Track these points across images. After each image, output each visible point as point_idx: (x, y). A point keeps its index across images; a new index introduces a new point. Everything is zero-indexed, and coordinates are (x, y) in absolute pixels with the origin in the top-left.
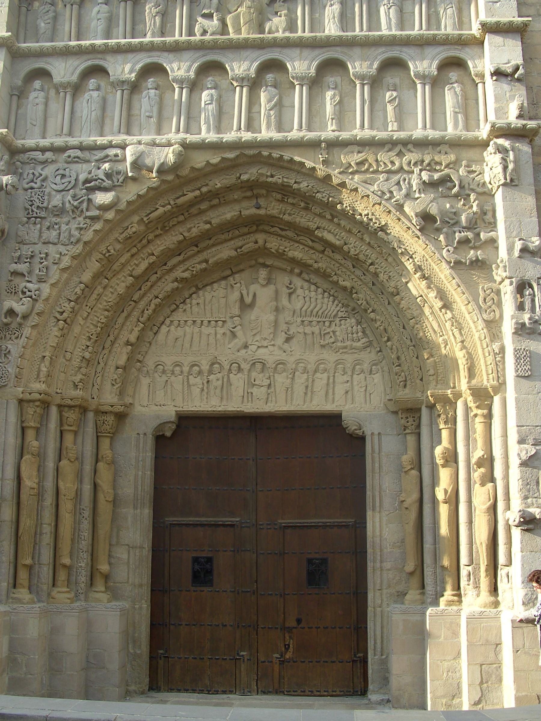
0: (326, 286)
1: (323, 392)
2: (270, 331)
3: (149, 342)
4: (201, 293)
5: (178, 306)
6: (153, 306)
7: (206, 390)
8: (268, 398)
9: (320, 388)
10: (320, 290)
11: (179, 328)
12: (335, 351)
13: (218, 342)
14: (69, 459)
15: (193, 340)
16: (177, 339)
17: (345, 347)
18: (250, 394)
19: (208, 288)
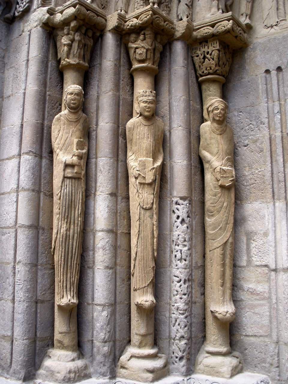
14: (141, 115)
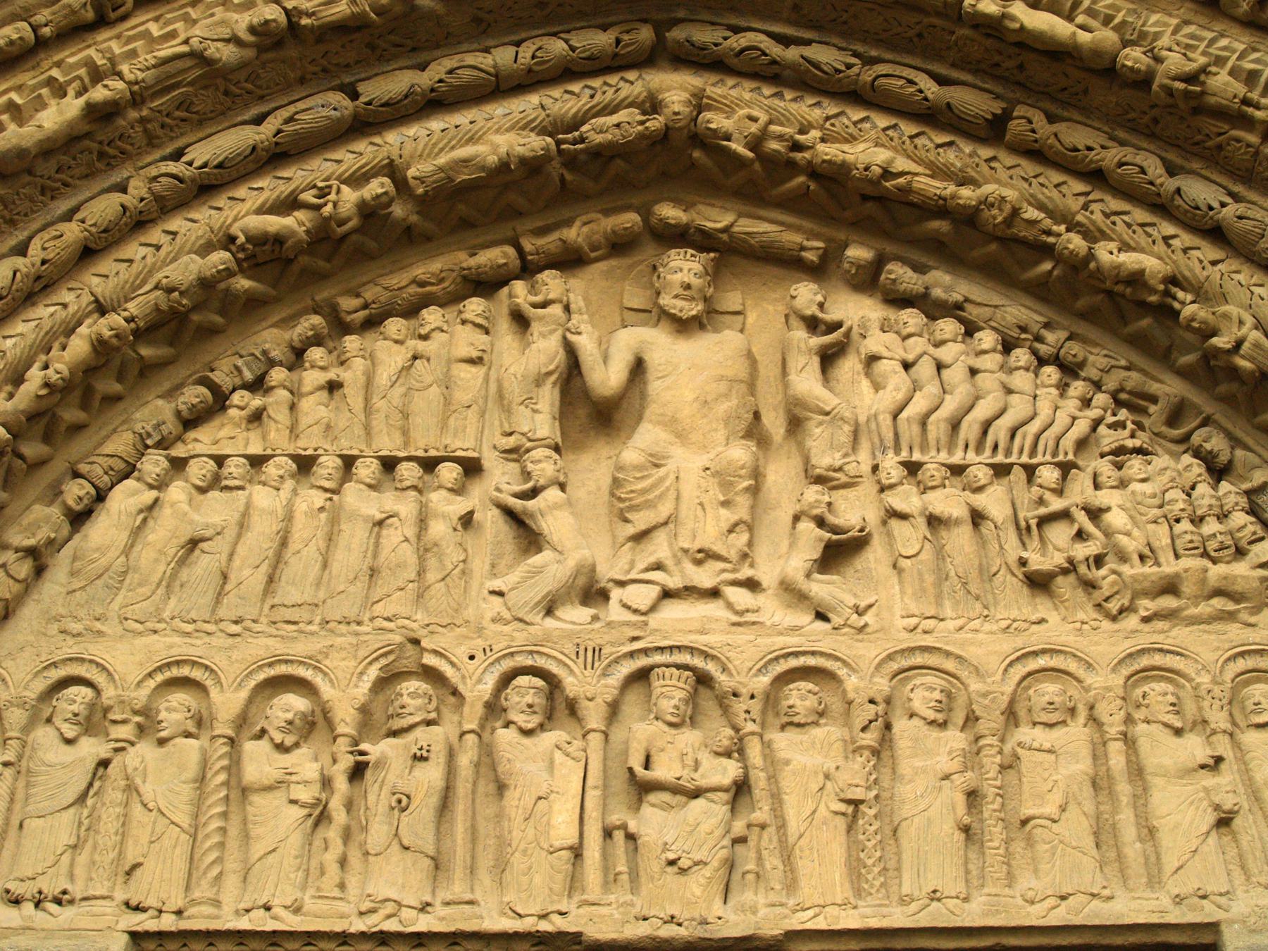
0: (1016, 311)
1: (1076, 827)
2: (727, 516)
3: (32, 552)
4: (351, 342)
5: (220, 401)
6: (79, 346)
7: (339, 815)
8: (730, 865)
9: (1057, 798)
10: (987, 339)
11: (214, 494)
12: (1113, 606)
13: (432, 562)
15: (288, 554)
16: (194, 544)
17: (1170, 587)
18: (619, 836)
19: (394, 326)
